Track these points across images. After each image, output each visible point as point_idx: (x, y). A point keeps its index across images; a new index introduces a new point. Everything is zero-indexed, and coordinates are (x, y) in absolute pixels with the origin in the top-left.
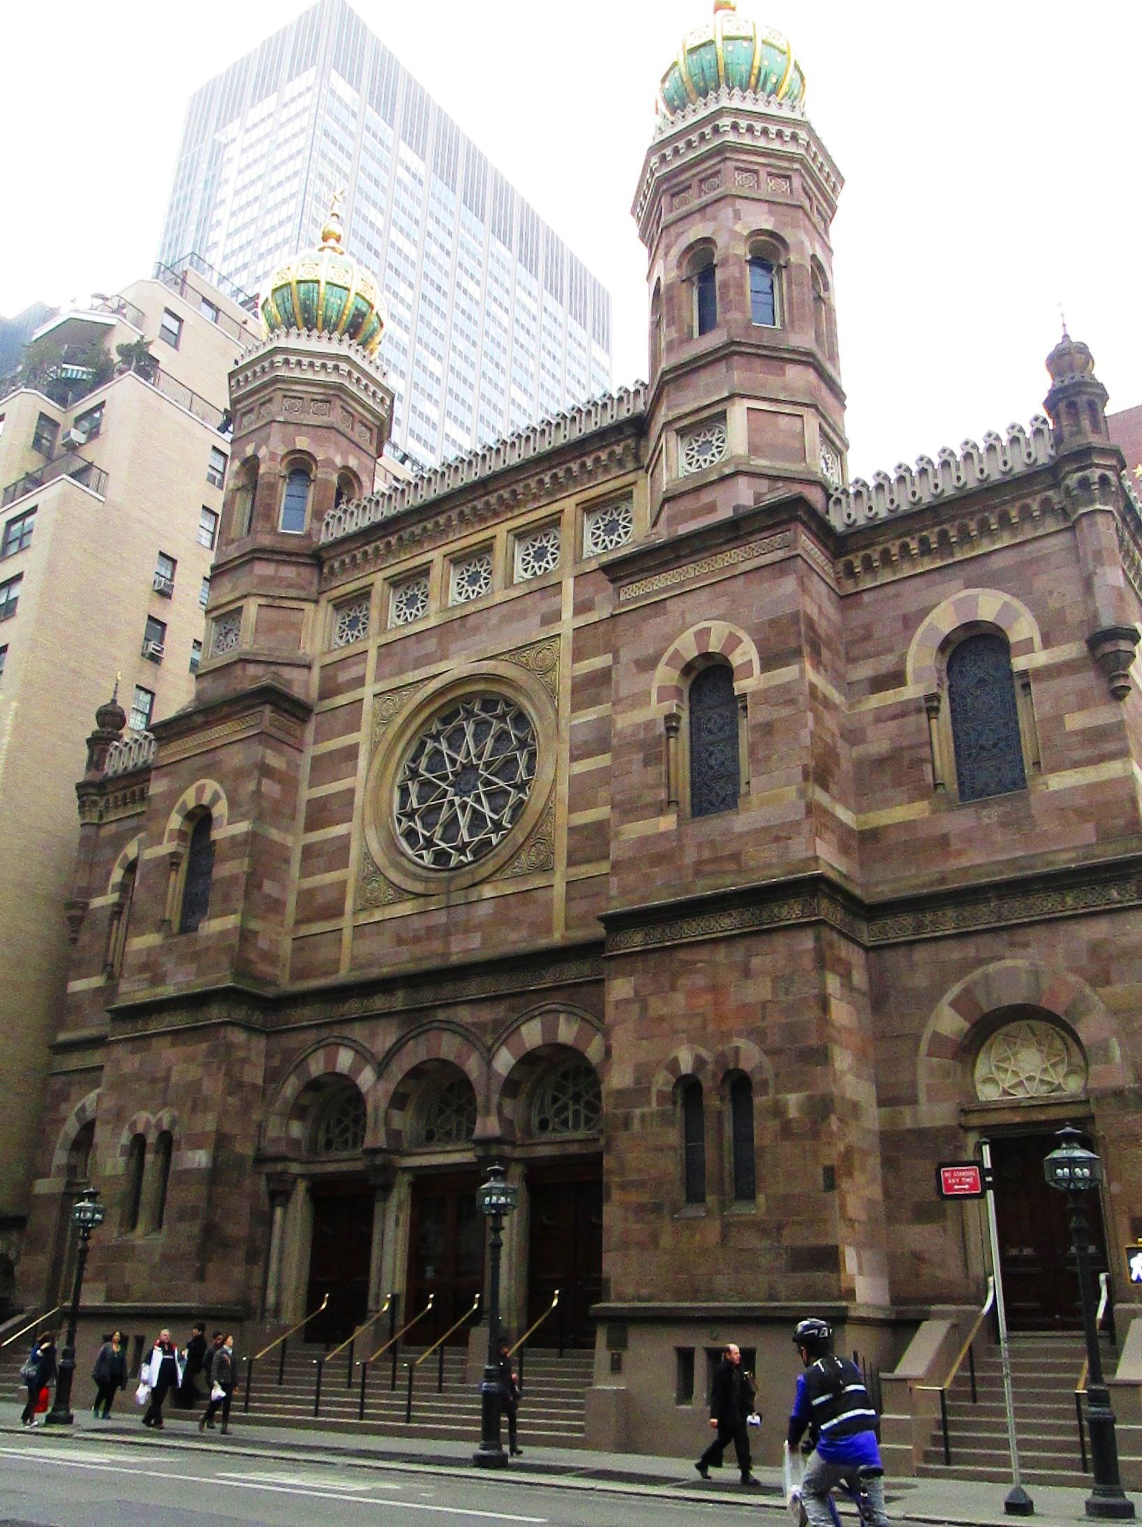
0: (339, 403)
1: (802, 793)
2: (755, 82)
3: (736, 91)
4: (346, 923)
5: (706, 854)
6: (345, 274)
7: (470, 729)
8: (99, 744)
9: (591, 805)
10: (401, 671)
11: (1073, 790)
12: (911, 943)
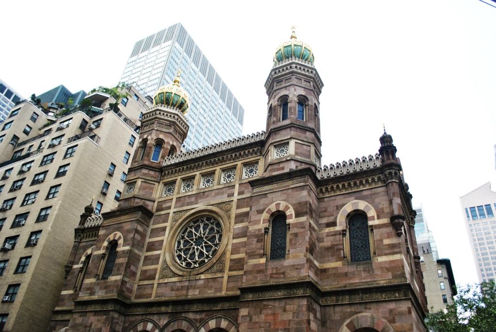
0: (173, 127)
1: (305, 256)
2: (302, 57)
3: (297, 58)
4: (156, 282)
5: (274, 272)
6: (181, 92)
7: (202, 226)
8: (84, 218)
9: (238, 253)
10: (183, 206)
11: (385, 262)
12: (334, 306)
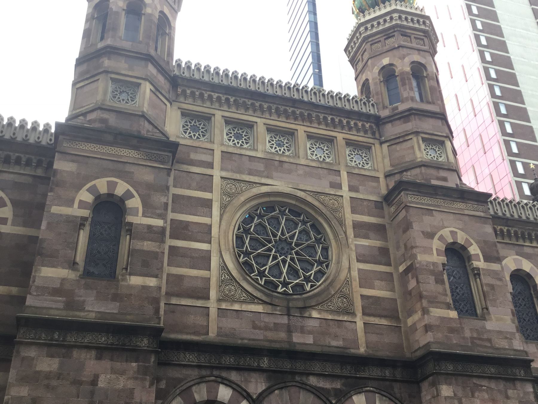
9: (372, 287)
